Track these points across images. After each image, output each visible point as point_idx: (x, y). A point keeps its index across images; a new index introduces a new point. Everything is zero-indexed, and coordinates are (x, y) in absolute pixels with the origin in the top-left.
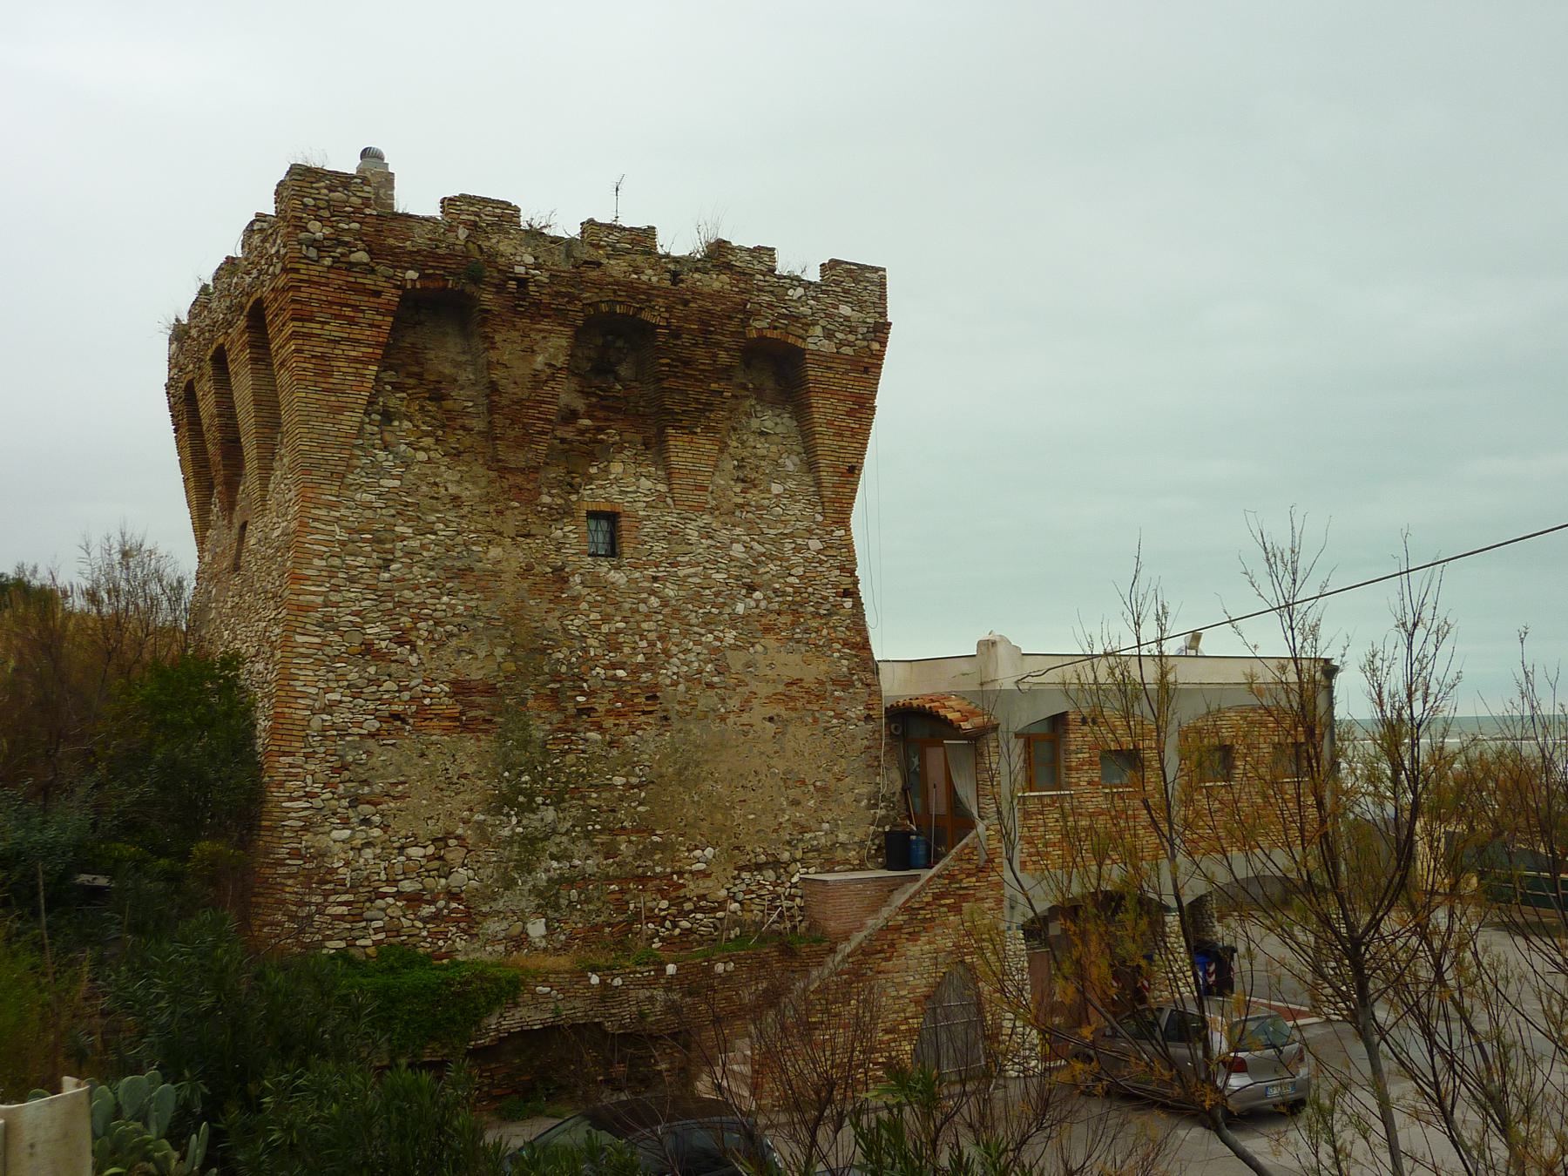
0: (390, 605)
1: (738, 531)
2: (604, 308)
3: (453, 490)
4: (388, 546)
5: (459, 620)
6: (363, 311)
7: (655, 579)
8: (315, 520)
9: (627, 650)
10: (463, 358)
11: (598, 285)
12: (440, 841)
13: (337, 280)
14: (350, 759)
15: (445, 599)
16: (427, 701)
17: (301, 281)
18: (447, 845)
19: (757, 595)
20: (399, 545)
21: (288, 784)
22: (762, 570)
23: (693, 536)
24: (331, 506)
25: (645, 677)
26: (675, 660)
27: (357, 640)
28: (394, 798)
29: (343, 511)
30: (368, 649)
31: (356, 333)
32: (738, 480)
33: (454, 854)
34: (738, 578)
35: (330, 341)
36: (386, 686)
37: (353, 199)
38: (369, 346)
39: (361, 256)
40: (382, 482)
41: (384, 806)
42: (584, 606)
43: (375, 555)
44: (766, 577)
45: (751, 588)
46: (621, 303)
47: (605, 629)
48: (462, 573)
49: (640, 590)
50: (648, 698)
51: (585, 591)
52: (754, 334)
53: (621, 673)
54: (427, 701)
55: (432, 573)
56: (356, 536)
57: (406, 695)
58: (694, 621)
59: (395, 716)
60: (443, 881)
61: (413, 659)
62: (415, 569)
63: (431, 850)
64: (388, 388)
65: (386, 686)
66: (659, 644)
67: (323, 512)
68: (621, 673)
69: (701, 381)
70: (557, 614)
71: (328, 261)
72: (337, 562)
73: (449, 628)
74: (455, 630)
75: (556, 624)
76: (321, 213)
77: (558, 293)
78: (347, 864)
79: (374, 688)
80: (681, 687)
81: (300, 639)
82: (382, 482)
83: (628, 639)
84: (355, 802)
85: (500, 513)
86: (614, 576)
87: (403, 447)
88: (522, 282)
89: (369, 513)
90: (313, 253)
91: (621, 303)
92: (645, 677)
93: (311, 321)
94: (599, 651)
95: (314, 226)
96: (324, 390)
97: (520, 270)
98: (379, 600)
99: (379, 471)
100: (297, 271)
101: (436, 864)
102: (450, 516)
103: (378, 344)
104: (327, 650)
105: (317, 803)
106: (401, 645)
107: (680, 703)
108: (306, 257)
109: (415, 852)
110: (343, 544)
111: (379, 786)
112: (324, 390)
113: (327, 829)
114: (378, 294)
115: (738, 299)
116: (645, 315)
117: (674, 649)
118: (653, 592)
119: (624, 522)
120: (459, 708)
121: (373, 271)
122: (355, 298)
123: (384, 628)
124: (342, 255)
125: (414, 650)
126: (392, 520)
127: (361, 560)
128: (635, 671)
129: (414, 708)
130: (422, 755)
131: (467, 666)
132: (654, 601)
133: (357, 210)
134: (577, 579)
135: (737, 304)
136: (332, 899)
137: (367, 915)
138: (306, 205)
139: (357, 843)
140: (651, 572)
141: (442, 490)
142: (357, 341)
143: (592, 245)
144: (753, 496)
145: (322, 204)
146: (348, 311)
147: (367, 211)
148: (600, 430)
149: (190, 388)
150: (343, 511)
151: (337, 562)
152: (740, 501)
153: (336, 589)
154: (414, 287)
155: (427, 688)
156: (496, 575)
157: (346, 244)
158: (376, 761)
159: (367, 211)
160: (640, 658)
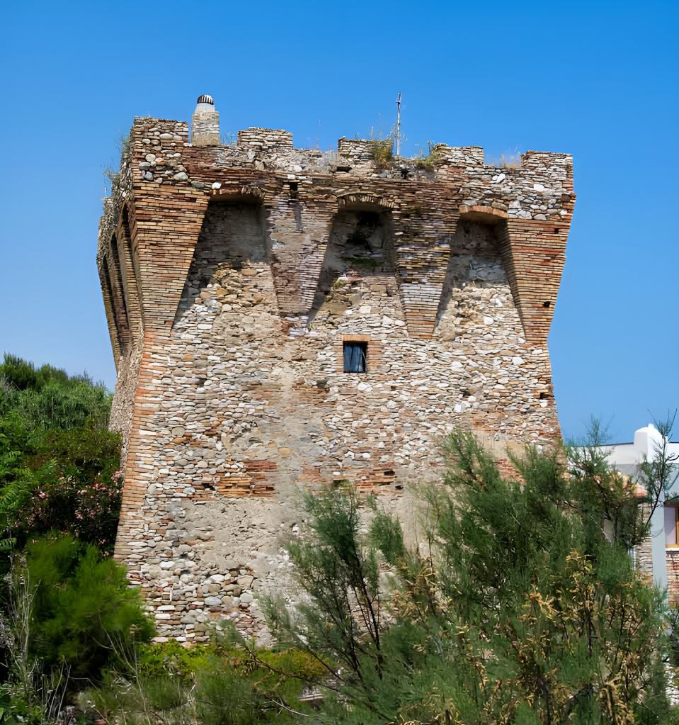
0: (204, 409)
1: (458, 352)
2: (352, 198)
3: (248, 330)
4: (204, 369)
5: (251, 419)
6: (184, 212)
7: (393, 388)
8: (153, 353)
9: (371, 439)
10: (257, 239)
11: (350, 184)
12: (235, 571)
13: (167, 191)
14: (174, 513)
15: (242, 405)
16: (228, 475)
17: (142, 195)
18: (239, 573)
19: (471, 398)
20: (210, 368)
21: (132, 530)
22: (475, 380)
23: (423, 357)
24: (164, 344)
25: (384, 458)
26: (407, 445)
27: (180, 432)
28: (204, 540)
29: (173, 347)
30: (188, 440)
31: (179, 226)
32: (458, 315)
33: (244, 580)
34: (457, 386)
35: (162, 233)
36: (200, 464)
37: (176, 137)
38: (187, 235)
39: (181, 176)
40: (200, 326)
41: (197, 546)
42: (339, 408)
43: (194, 376)
44: (478, 385)
45: (466, 394)
46: (366, 195)
47: (355, 424)
48: (253, 387)
49: (382, 396)
50: (386, 473)
51: (340, 398)
52: (466, 210)
53: (366, 456)
54: (228, 475)
55: (233, 387)
56: (181, 363)
57: (213, 470)
58: (423, 418)
59: (206, 485)
60: (236, 599)
61: (219, 446)
62: (221, 385)
63: (228, 577)
64: (205, 262)
65: (200, 464)
66: (395, 435)
67: (159, 348)
68: (366, 456)
69: (427, 246)
70: (321, 414)
71: (160, 180)
72: (168, 381)
73: (244, 424)
74: (248, 426)
75: (320, 421)
76: (155, 148)
77: (320, 192)
78: (170, 585)
79: (192, 466)
80: (412, 466)
81: (142, 433)
82: (200, 326)
83: (371, 431)
84: (177, 542)
85: (280, 344)
86: (362, 386)
87: (215, 302)
88: (294, 186)
89: (190, 347)
90: (149, 175)
91: (366, 195)
92: (384, 458)
93: (149, 221)
94: (351, 440)
95: (150, 157)
96: (159, 266)
97: (291, 177)
98: (196, 405)
99: (197, 319)
100: (139, 188)
101: (231, 586)
102: (246, 348)
103: (194, 233)
104: (161, 440)
105: (151, 543)
106: (211, 436)
107: (410, 477)
108: (145, 179)
109: (218, 578)
110: (173, 369)
111: (194, 532)
112: (159, 266)
113: (157, 560)
114: (193, 200)
115: (452, 185)
116: (383, 202)
117: (407, 438)
118: (391, 398)
119: (370, 348)
120: (250, 479)
121: (190, 185)
122: (177, 204)
123: (199, 424)
124: (169, 175)
125: (219, 439)
126: (206, 352)
127: (184, 379)
128: (377, 454)
129: (218, 479)
130: (224, 511)
131: (255, 451)
132: (392, 404)
133: (178, 145)
134: (336, 389)
135: (452, 190)
136: (159, 608)
137: (184, 620)
138: (145, 144)
139: (178, 571)
140: (391, 383)
141: (242, 331)
142: (181, 232)
143: (344, 155)
144: (469, 326)
145: (155, 142)
146: (174, 213)
147: (185, 145)
148: (354, 284)
149: (105, 261)
150: (173, 347)
151: (168, 381)
152: (460, 330)
153: (167, 399)
154: (218, 193)
155: (228, 466)
156: (278, 387)
157: (171, 168)
158: (192, 515)
159: (185, 145)
160: (381, 445)
